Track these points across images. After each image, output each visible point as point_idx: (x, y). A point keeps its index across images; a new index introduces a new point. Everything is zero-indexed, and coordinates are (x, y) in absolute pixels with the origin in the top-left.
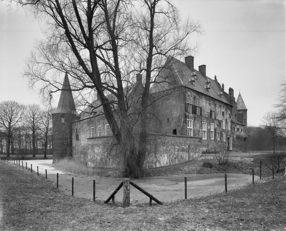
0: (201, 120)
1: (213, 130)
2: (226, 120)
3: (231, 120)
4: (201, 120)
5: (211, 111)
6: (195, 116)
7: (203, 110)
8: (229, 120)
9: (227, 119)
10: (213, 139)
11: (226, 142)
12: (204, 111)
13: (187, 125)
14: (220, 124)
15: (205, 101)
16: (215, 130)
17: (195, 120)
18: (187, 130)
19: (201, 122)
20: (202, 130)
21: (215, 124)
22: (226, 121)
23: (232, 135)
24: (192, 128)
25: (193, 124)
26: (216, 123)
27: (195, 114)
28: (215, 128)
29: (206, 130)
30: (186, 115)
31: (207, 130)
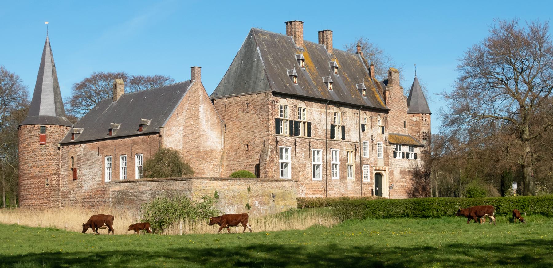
0: (310, 145)
1: (338, 162)
2: (372, 139)
3: (384, 139)
4: (310, 145)
5: (333, 127)
6: (295, 139)
7: (312, 127)
8: (379, 139)
9: (375, 136)
10: (338, 178)
11: (369, 184)
12: (316, 129)
13: (279, 157)
14: (355, 149)
15: (319, 110)
16: (344, 161)
17: (295, 147)
18: (278, 166)
19: (310, 150)
20: (311, 164)
21: (341, 149)
22: (372, 142)
23: (389, 169)
24: (289, 161)
25: (292, 154)
26: (344, 148)
27: (297, 134)
28: (343, 157)
29: (321, 162)
30: (277, 140)
31: (323, 162)
